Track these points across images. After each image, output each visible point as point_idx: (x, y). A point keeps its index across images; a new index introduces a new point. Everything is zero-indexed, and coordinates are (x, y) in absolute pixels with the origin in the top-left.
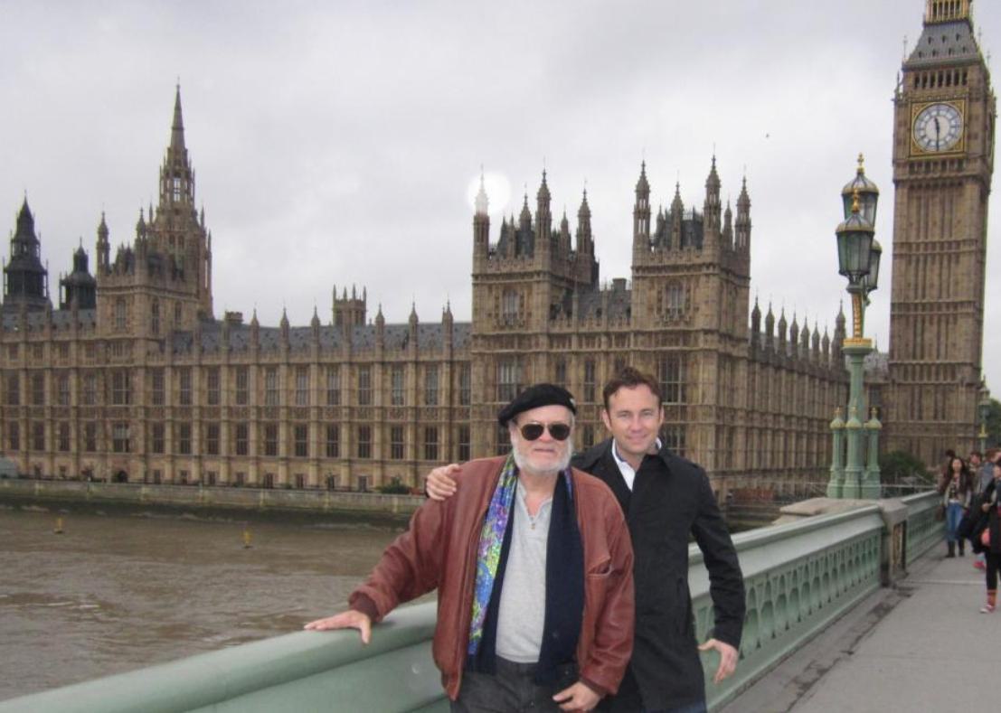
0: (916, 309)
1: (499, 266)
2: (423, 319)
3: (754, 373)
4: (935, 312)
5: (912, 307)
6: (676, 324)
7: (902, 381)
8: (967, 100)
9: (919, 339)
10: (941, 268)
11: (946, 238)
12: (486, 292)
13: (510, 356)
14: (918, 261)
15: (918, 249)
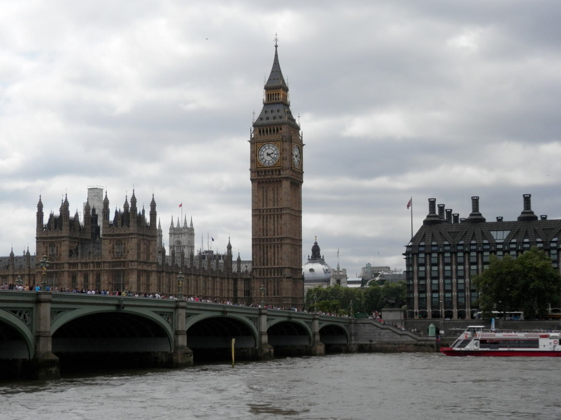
0: (263, 241)
1: (47, 234)
2: (16, 254)
3: (163, 277)
4: (272, 242)
5: (262, 240)
6: (120, 258)
7: (258, 277)
8: (281, 142)
9: (265, 256)
10: (274, 221)
11: (276, 207)
12: (42, 243)
13: (53, 272)
14: (263, 218)
15: (263, 212)
